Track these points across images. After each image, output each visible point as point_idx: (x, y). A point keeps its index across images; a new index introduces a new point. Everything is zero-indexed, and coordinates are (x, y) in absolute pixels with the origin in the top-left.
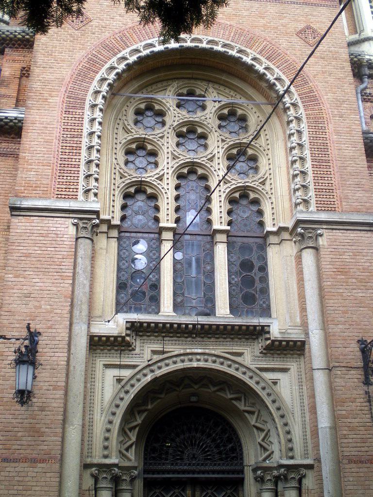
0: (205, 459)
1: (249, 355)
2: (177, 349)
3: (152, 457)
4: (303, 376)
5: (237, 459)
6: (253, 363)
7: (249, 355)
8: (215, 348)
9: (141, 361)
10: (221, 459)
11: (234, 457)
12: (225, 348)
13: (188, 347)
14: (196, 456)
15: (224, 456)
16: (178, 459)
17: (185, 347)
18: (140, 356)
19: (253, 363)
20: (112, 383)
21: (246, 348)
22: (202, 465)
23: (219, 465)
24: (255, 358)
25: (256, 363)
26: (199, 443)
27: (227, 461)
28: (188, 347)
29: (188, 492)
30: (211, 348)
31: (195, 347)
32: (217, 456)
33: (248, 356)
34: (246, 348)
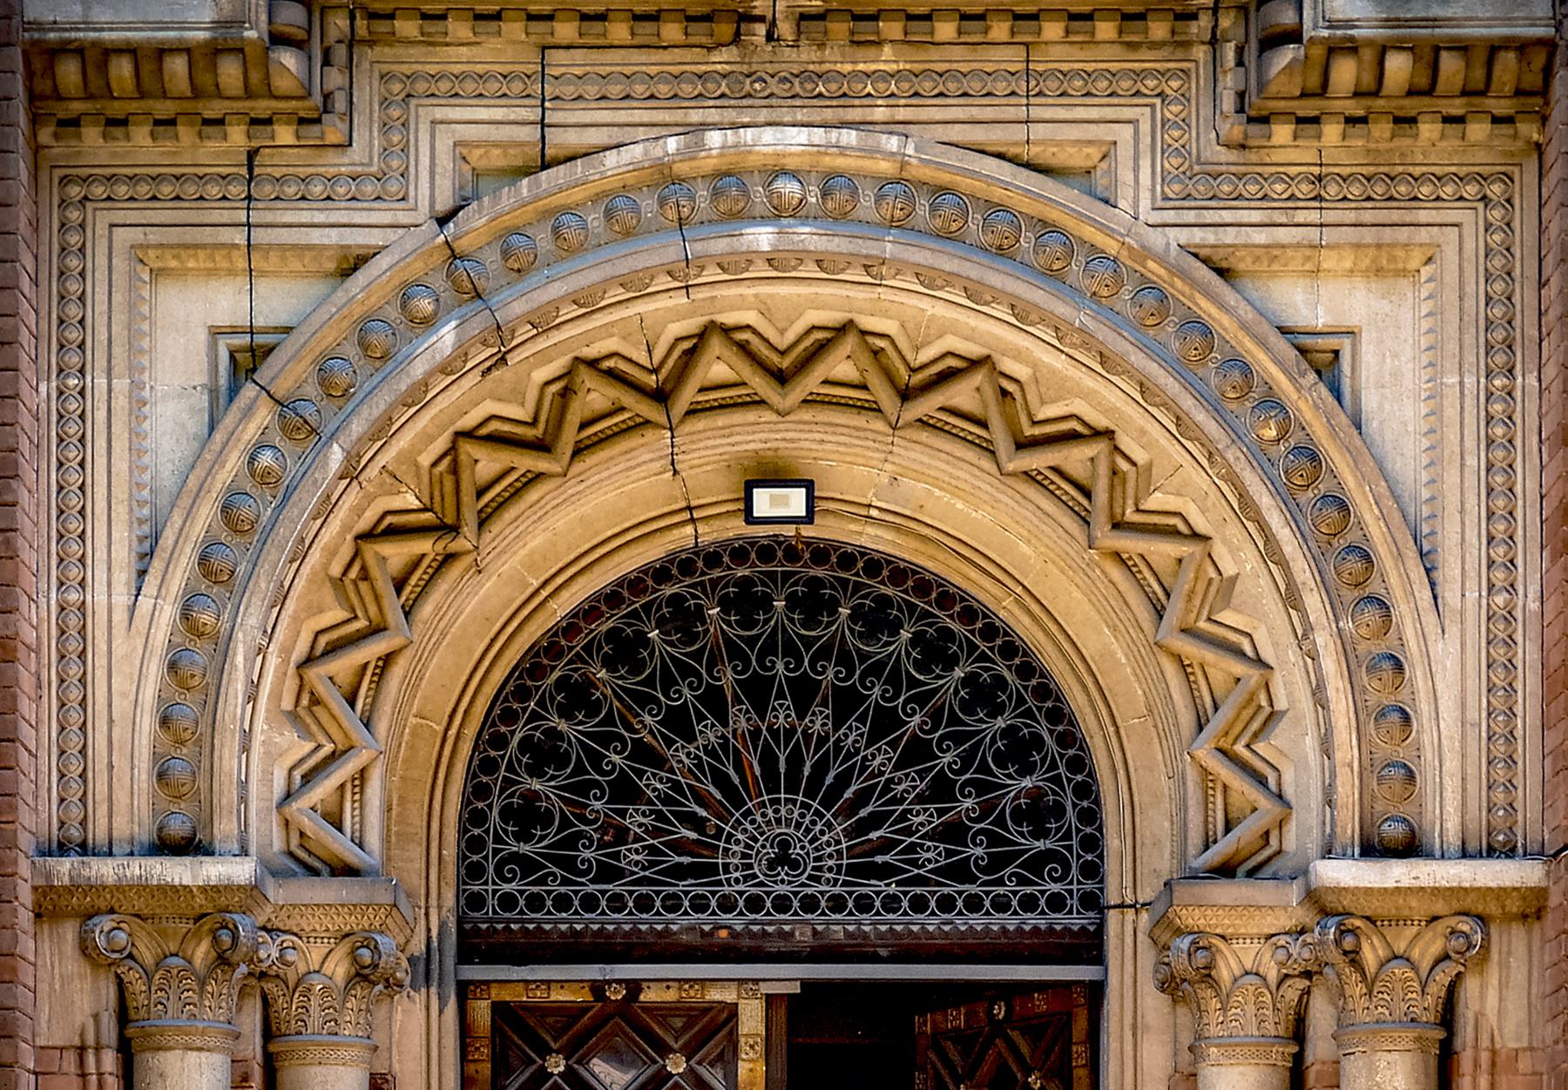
0: (852, 870)
1: (1145, 165)
2: (641, 133)
3: (515, 857)
4: (1525, 296)
5: (1067, 868)
6: (1170, 216)
7: (1145, 165)
8: (902, 114)
9: (386, 218)
10: (960, 872)
11: (1049, 855)
12: (976, 113)
13: (713, 116)
14: (795, 851)
15: (979, 851)
16: (679, 872)
17: (695, 116)
18: (386, 184)
19: (1170, 216)
20: (202, 378)
21: (1128, 113)
22: (837, 904)
23: (946, 904)
24: (1193, 186)
25: (1190, 217)
26: (821, 768)
27: (1000, 882)
28: (713, 116)
29: (743, 1068)
30: (880, 114)
31: (763, 115)
32: (932, 855)
33: (1136, 169)
34: (1128, 113)
